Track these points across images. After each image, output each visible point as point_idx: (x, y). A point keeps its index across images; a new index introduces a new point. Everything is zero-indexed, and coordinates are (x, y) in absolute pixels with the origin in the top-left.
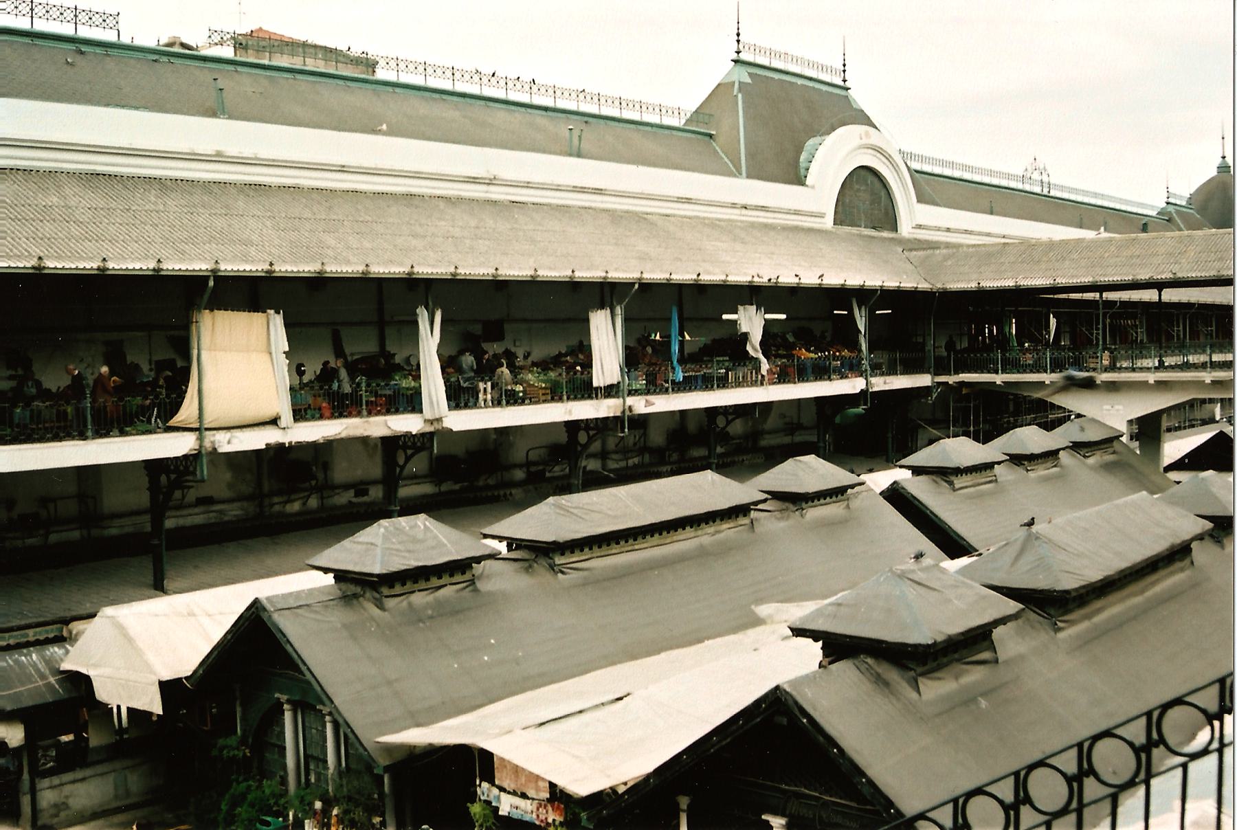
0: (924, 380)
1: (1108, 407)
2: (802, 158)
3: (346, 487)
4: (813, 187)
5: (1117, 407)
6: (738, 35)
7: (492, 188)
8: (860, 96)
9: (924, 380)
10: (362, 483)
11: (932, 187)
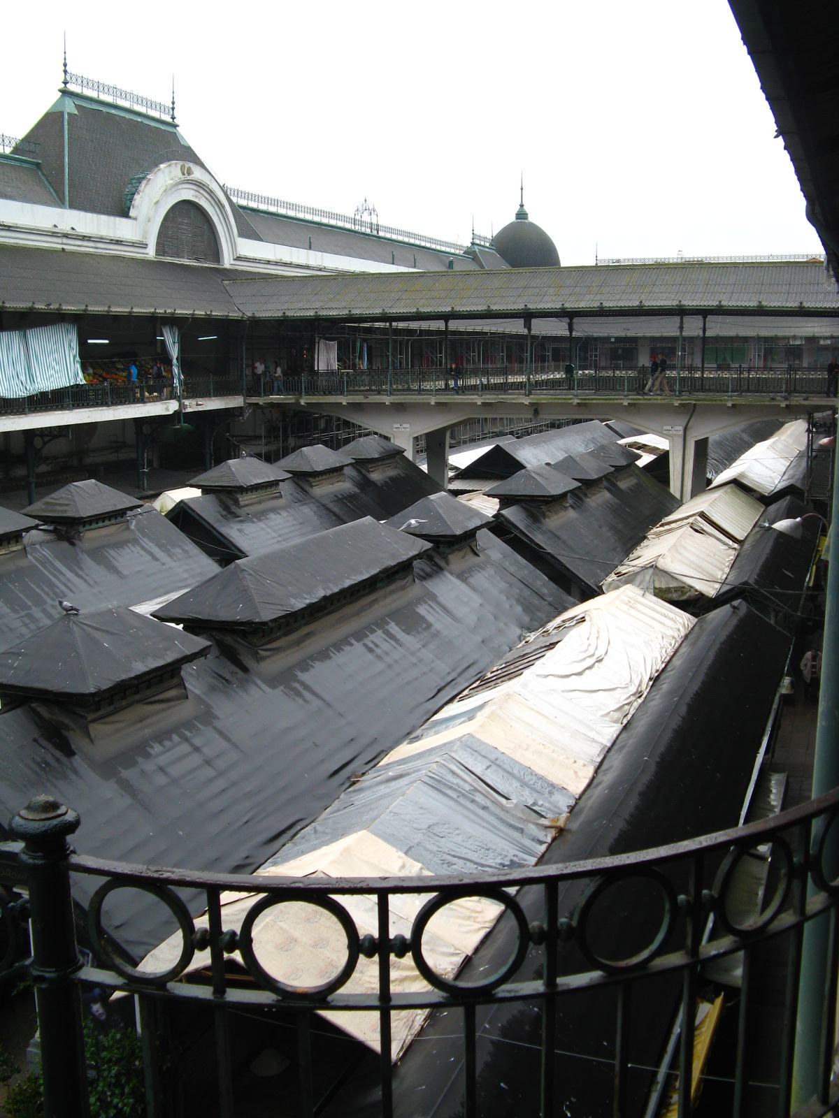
0: (235, 402)
4: (135, 219)
5: (405, 425)
6: (65, 65)
8: (189, 133)
9: (235, 402)
11: (254, 221)
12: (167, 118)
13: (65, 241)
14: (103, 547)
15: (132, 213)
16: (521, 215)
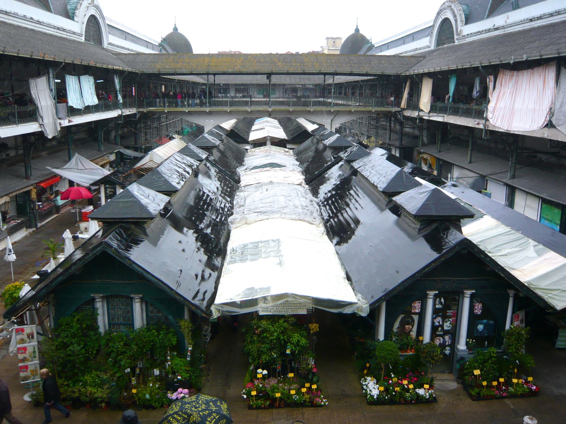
4: (78, 22)
13: (58, 31)
14: (454, 164)
15: (75, 19)
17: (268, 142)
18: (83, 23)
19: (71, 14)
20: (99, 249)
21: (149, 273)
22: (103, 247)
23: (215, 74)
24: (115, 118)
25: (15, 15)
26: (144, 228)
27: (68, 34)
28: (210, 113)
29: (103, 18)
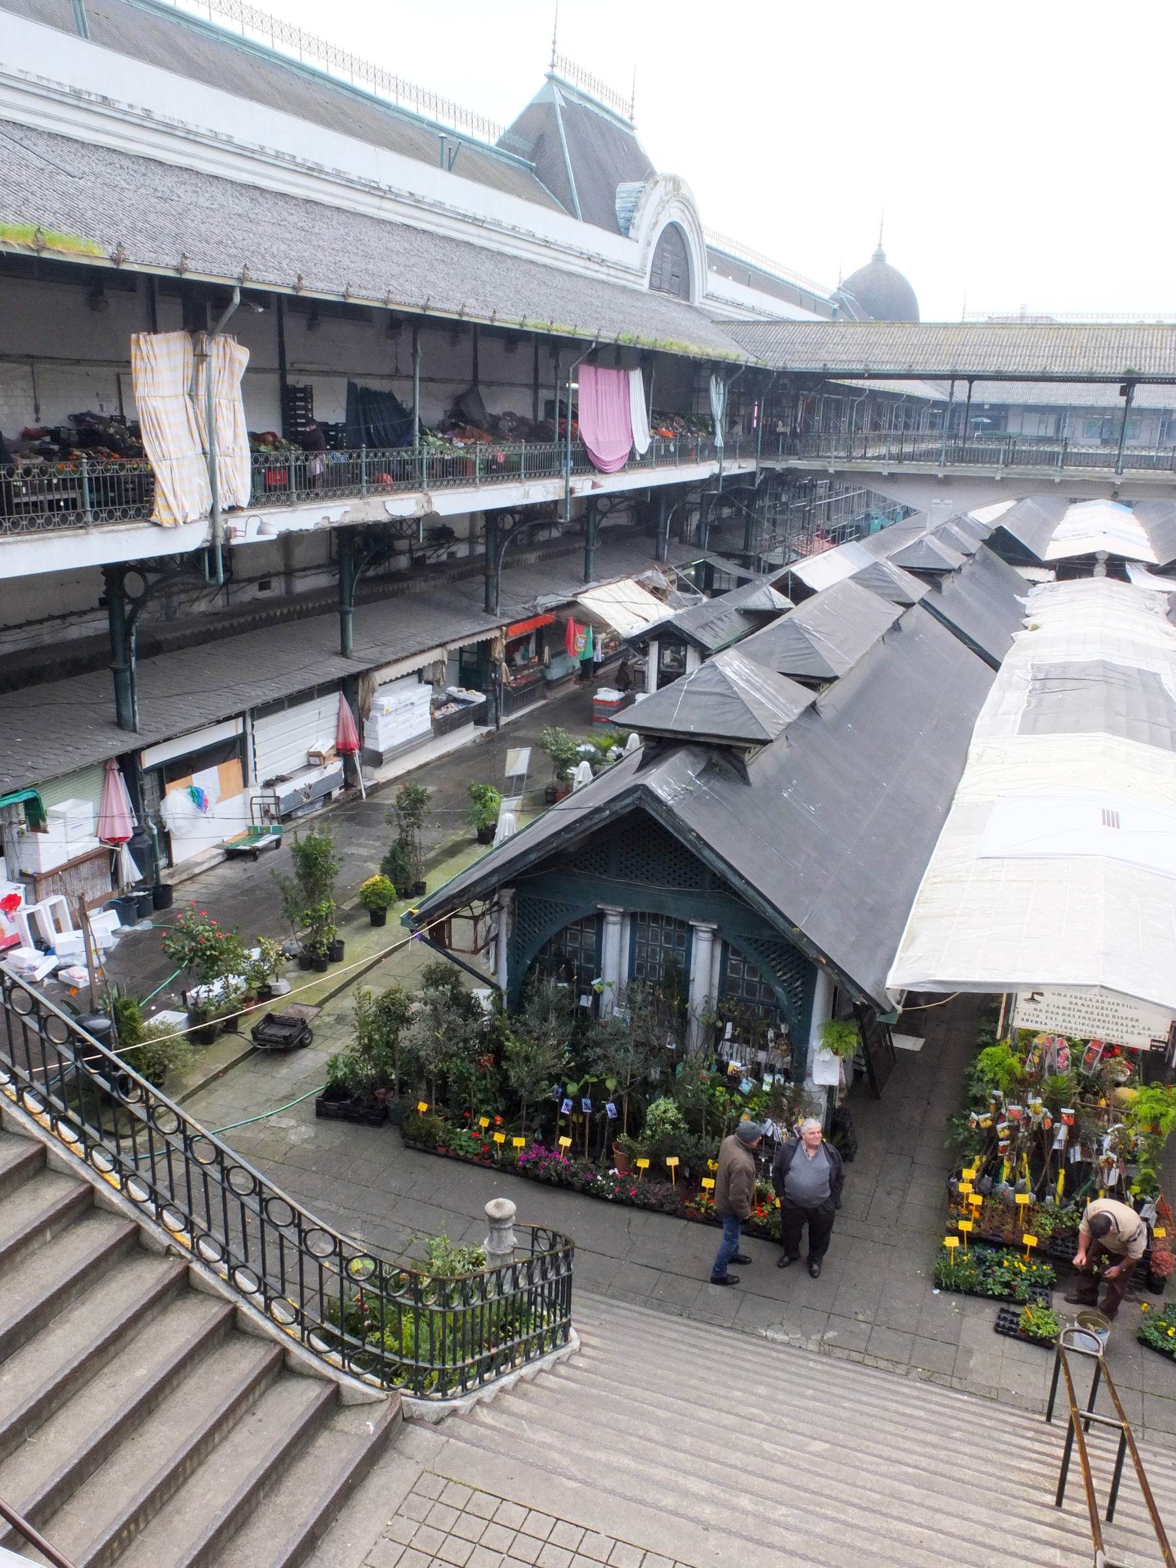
1: (938, 501)
2: (619, 204)
3: (250, 580)
5: (947, 501)
6: (554, 43)
7: (386, 204)
10: (264, 576)
12: (626, 118)
13: (588, 264)
15: (632, 232)
16: (879, 257)
17: (1100, 569)
18: (649, 244)
19: (621, 222)
20: (628, 801)
21: (742, 877)
22: (640, 798)
23: (971, 378)
24: (703, 481)
25: (495, 227)
26: (742, 762)
27: (612, 272)
28: (947, 481)
29: (699, 230)
